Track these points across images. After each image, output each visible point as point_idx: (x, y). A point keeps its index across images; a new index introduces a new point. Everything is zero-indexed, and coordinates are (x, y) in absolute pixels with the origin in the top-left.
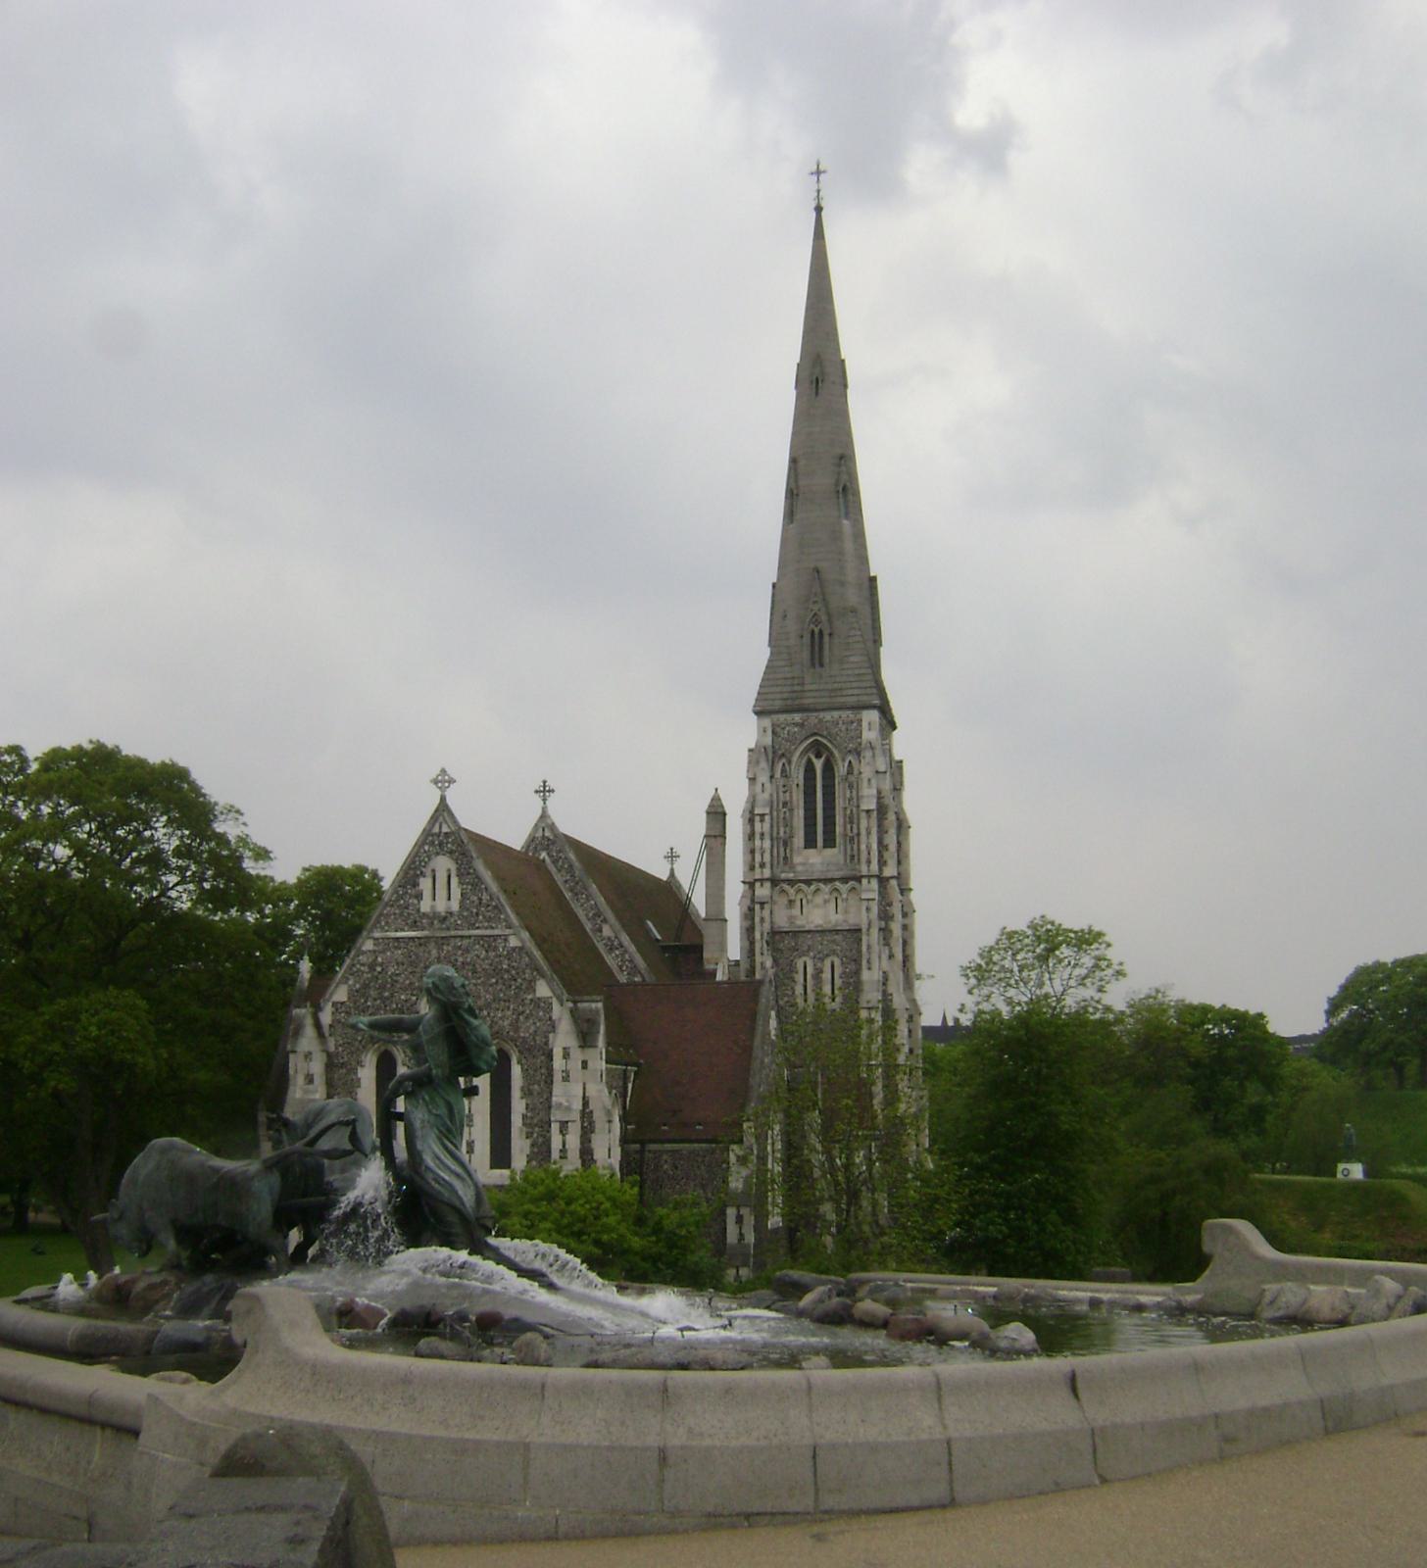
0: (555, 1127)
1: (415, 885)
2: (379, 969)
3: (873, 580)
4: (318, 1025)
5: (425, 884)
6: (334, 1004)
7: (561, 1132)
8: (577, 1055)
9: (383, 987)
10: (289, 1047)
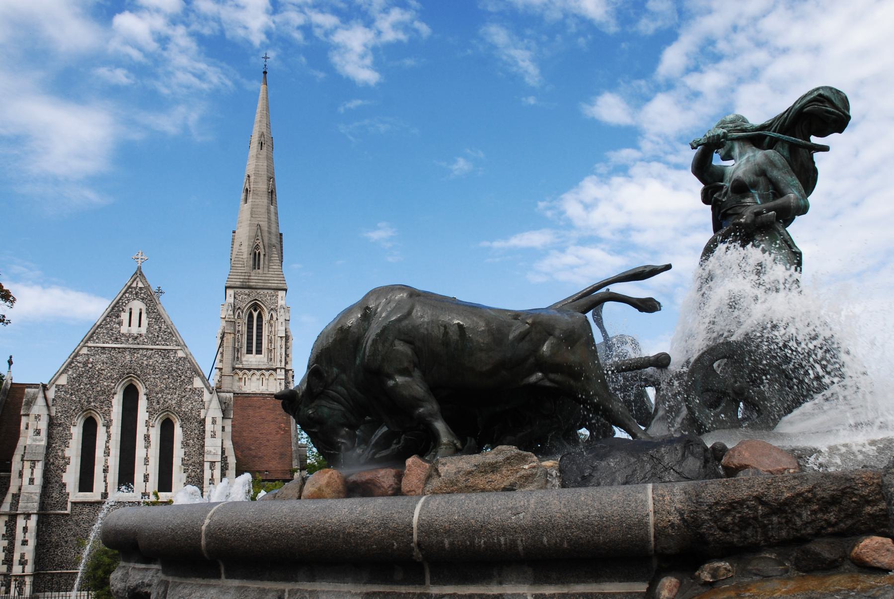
1: (118, 316)
2: (90, 365)
3: (281, 235)
4: (45, 398)
5: (125, 316)
6: (57, 386)
7: (211, 468)
9: (92, 377)
10: (22, 412)
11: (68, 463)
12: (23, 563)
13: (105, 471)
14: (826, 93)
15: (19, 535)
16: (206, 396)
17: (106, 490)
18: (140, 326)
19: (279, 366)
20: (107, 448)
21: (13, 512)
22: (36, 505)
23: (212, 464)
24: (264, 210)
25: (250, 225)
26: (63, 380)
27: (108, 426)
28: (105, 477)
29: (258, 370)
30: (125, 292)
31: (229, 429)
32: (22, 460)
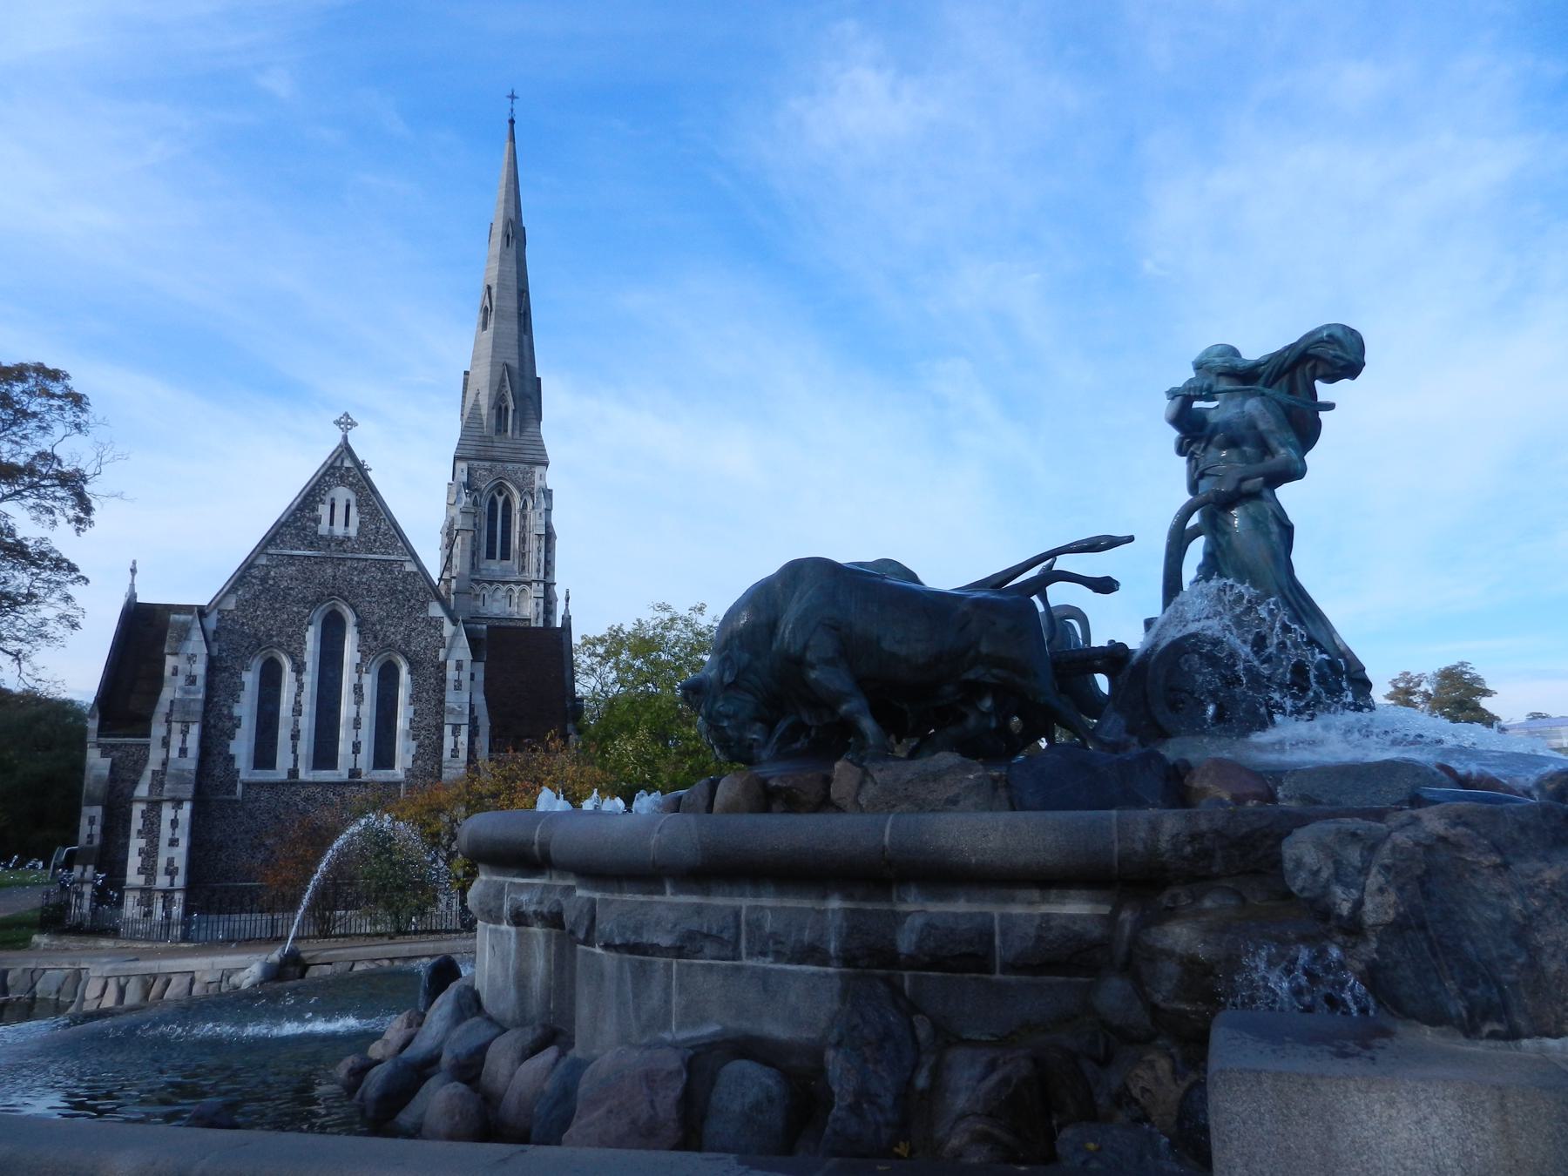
0: (448, 730)
1: (314, 510)
5: (323, 511)
8: (467, 665)
11: (238, 726)
12: (171, 871)
13: (295, 736)
14: (1339, 333)
15: (165, 831)
16: (448, 629)
17: (295, 765)
18: (347, 524)
19: (534, 577)
20: (298, 703)
21: (156, 798)
22: (191, 787)
23: (456, 729)
24: (514, 342)
25: (493, 364)
26: (231, 604)
27: (299, 669)
28: (295, 747)
29: (504, 583)
30: (325, 474)
31: (480, 677)
32: (169, 722)
